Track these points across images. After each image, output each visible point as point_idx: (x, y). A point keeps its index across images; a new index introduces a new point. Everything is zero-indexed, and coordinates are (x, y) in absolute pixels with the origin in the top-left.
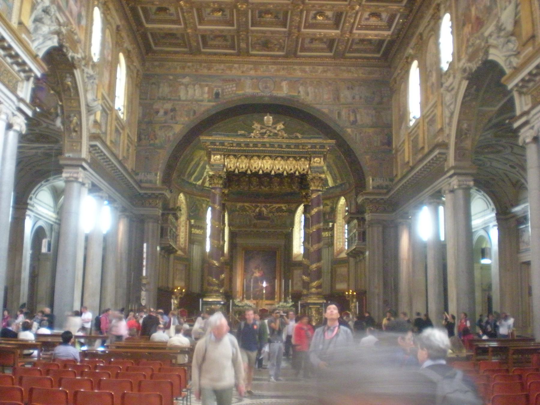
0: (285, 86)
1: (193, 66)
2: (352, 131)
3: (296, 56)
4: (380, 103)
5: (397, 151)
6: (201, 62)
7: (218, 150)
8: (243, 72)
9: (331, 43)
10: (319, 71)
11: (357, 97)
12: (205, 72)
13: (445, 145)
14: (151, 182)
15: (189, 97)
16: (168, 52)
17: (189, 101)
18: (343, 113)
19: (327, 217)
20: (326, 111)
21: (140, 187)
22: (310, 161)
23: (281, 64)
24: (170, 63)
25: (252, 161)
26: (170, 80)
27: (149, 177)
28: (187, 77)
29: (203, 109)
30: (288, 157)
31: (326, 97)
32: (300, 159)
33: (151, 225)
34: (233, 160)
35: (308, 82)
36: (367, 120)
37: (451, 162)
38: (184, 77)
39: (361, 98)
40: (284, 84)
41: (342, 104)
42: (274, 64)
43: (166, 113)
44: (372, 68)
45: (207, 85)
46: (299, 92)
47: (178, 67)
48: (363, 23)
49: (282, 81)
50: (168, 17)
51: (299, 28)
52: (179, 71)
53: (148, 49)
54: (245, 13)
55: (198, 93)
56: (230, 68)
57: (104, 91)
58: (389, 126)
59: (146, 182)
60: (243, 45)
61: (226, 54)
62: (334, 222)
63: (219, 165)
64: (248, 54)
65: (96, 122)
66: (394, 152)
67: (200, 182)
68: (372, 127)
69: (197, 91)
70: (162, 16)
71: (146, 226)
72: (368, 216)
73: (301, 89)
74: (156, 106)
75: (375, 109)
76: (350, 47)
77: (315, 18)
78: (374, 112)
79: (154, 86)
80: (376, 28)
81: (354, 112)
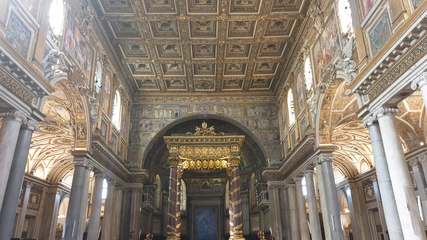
0: (215, 108)
1: (162, 99)
2: (256, 133)
3: (221, 91)
4: (271, 116)
5: (283, 143)
6: (167, 96)
10: (235, 99)
11: (257, 113)
15: (160, 116)
16: (148, 91)
17: (161, 118)
18: (250, 122)
20: (240, 121)
23: (213, 96)
24: (149, 98)
26: (149, 107)
28: (159, 105)
29: (168, 123)
31: (239, 113)
35: (229, 106)
36: (264, 126)
38: (157, 106)
40: (215, 107)
41: (249, 117)
42: (208, 96)
44: (265, 96)
45: (171, 109)
46: (224, 111)
47: (154, 100)
49: (214, 105)
50: (146, 70)
52: (154, 102)
58: (278, 129)
61: (181, 92)
64: (194, 91)
69: (165, 113)
70: (142, 69)
75: (268, 119)
76: (252, 85)
77: (230, 68)
78: (268, 121)
79: (139, 111)
81: (256, 121)
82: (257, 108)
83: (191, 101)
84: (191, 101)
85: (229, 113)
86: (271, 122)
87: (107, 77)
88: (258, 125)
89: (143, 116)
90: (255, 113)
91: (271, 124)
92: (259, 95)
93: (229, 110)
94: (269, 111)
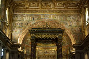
5: (83, 33)
7: (33, 32)
11: (71, 19)
14: (15, 42)
15: (26, 20)
16: (20, 8)
18: (68, 23)
19: (65, 52)
22: (58, 35)
25: (42, 35)
30: (52, 34)
32: (55, 35)
33: (15, 54)
34: (37, 35)
38: (25, 14)
39: (72, 19)
40: (51, 16)
41: (67, 21)
43: (20, 24)
45: (31, 17)
49: (51, 15)
56: (37, 12)
57: (2, 17)
63: (33, 37)
66: (82, 33)
71: (14, 54)
73: (56, 17)
75: (76, 22)
78: (76, 22)
81: (70, 22)
82: (71, 16)
83: (40, 13)
85: (58, 18)
86: (78, 23)
87: (3, 2)
89: (18, 19)
90: (70, 19)
91: (78, 24)
92: (73, 10)
93: (58, 17)
94: (77, 18)
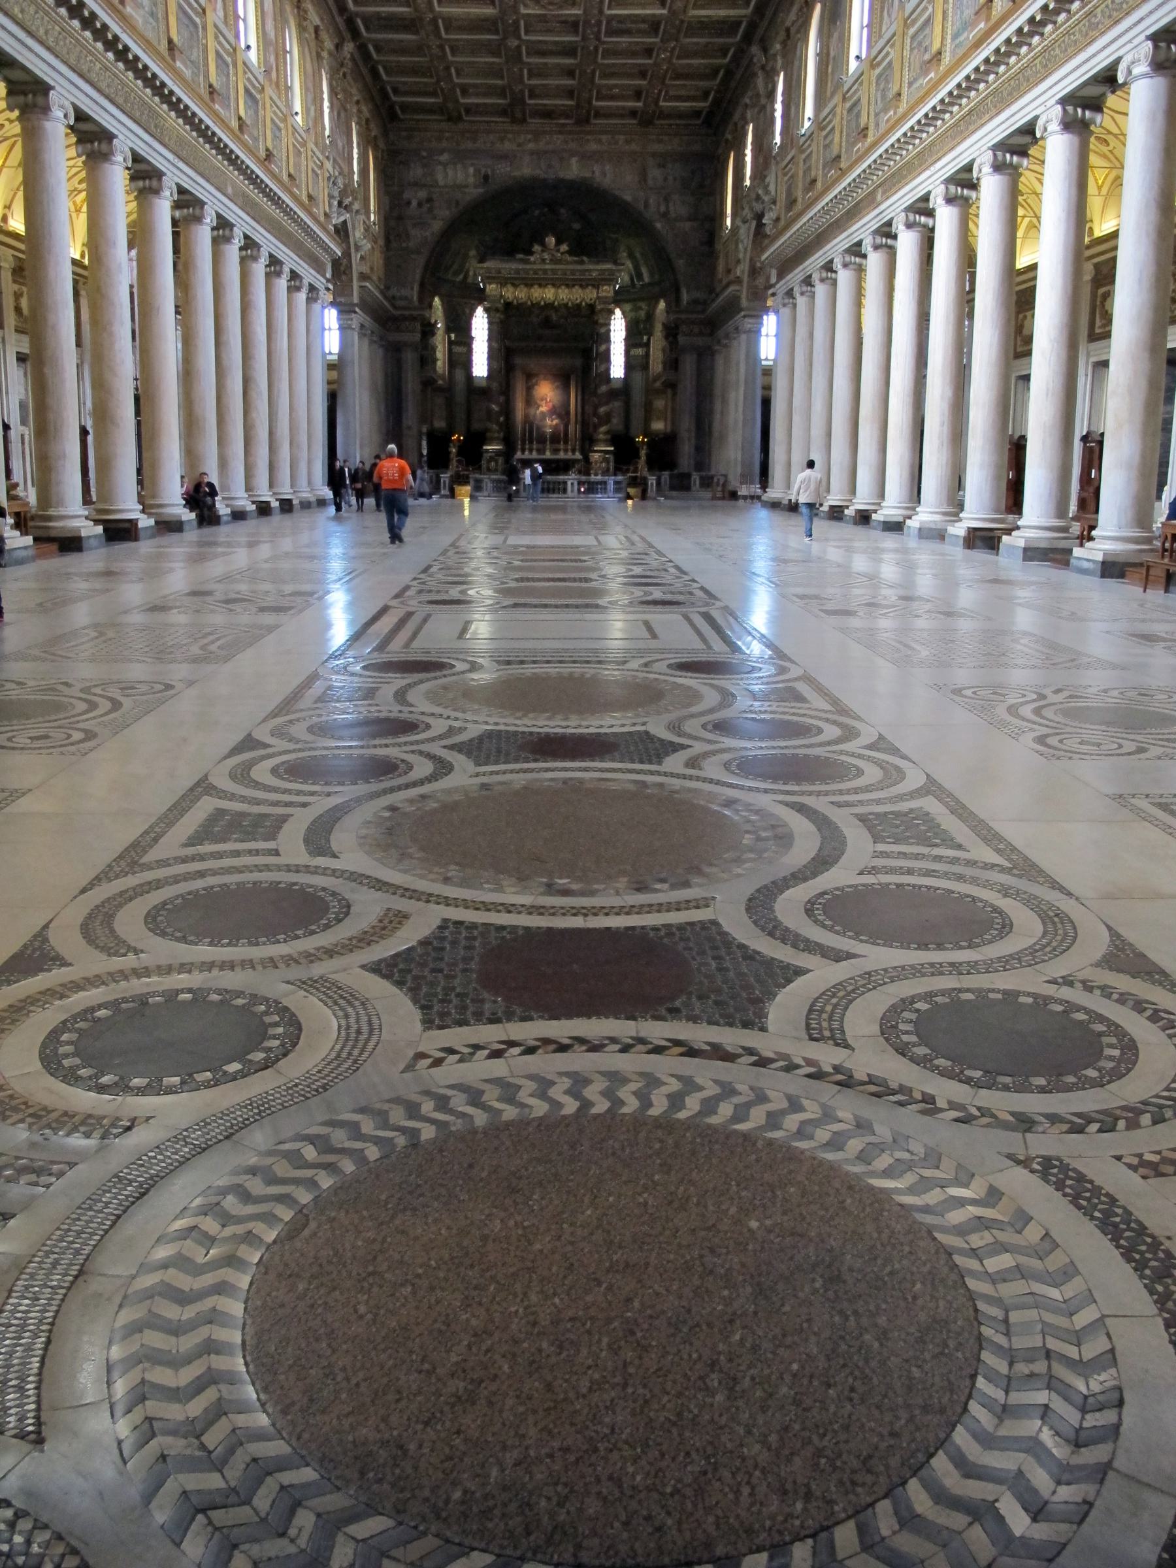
8: (519, 145)
9: (633, 113)
11: (671, 178)
12: (469, 145)
13: (738, 280)
14: (406, 298)
20: (628, 198)
21: (395, 307)
23: (570, 133)
27: (404, 292)
29: (468, 198)
34: (511, 289)
36: (683, 211)
37: (744, 302)
38: (442, 152)
40: (574, 160)
42: (560, 133)
43: (420, 205)
48: (671, 93)
51: (590, 102)
53: (393, 117)
54: (522, 92)
55: (460, 176)
56: (502, 140)
59: (401, 298)
60: (519, 115)
62: (650, 334)
64: (523, 121)
65: (362, 258)
67: (461, 277)
68: (689, 219)
72: (681, 339)
74: (406, 196)
80: (688, 99)
84: (519, 145)
85: (604, 174)
88: (671, 208)
